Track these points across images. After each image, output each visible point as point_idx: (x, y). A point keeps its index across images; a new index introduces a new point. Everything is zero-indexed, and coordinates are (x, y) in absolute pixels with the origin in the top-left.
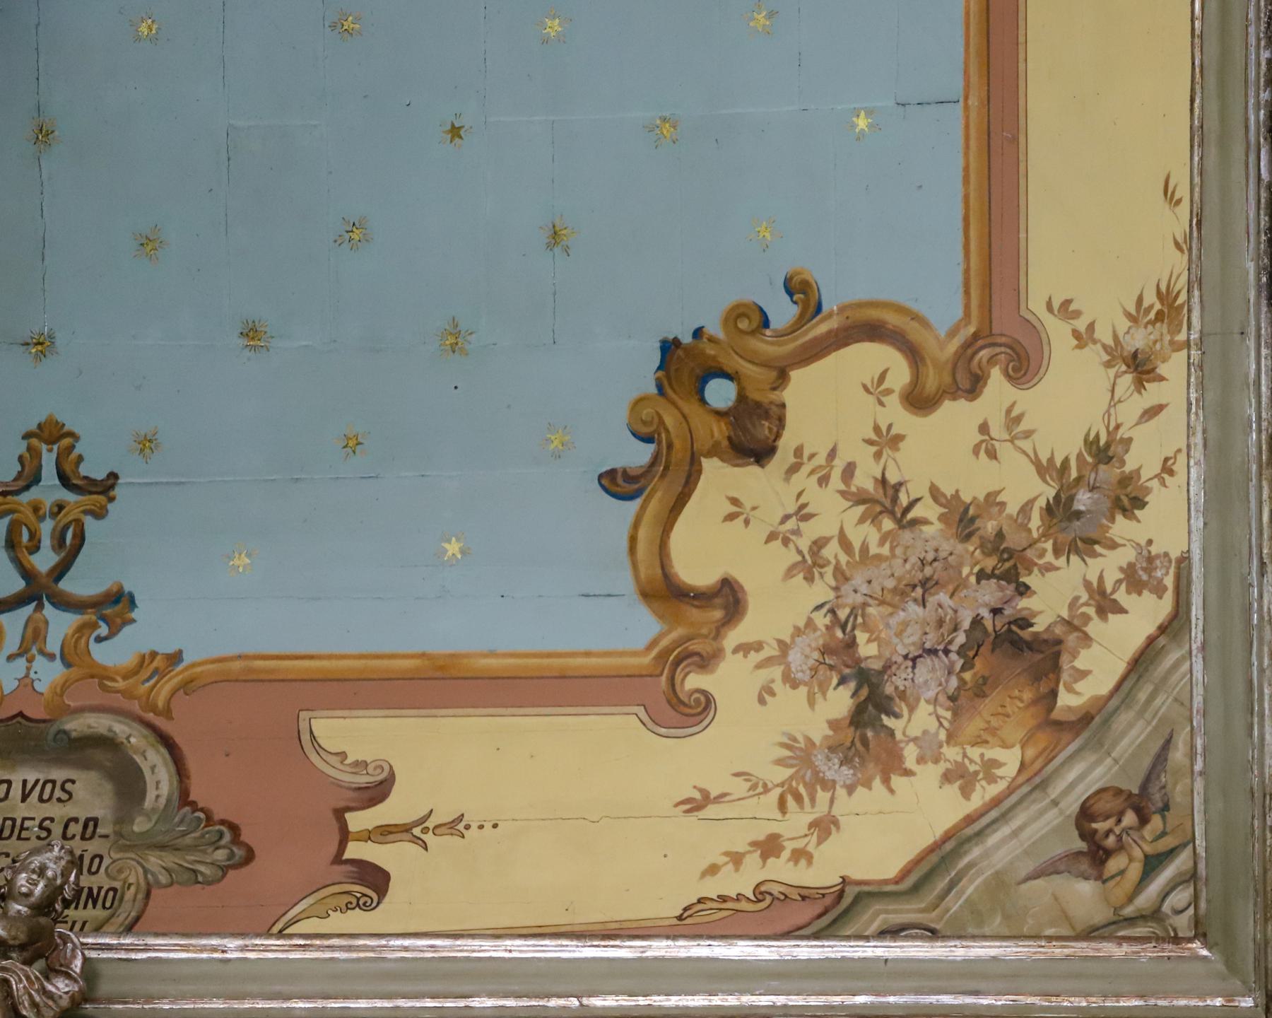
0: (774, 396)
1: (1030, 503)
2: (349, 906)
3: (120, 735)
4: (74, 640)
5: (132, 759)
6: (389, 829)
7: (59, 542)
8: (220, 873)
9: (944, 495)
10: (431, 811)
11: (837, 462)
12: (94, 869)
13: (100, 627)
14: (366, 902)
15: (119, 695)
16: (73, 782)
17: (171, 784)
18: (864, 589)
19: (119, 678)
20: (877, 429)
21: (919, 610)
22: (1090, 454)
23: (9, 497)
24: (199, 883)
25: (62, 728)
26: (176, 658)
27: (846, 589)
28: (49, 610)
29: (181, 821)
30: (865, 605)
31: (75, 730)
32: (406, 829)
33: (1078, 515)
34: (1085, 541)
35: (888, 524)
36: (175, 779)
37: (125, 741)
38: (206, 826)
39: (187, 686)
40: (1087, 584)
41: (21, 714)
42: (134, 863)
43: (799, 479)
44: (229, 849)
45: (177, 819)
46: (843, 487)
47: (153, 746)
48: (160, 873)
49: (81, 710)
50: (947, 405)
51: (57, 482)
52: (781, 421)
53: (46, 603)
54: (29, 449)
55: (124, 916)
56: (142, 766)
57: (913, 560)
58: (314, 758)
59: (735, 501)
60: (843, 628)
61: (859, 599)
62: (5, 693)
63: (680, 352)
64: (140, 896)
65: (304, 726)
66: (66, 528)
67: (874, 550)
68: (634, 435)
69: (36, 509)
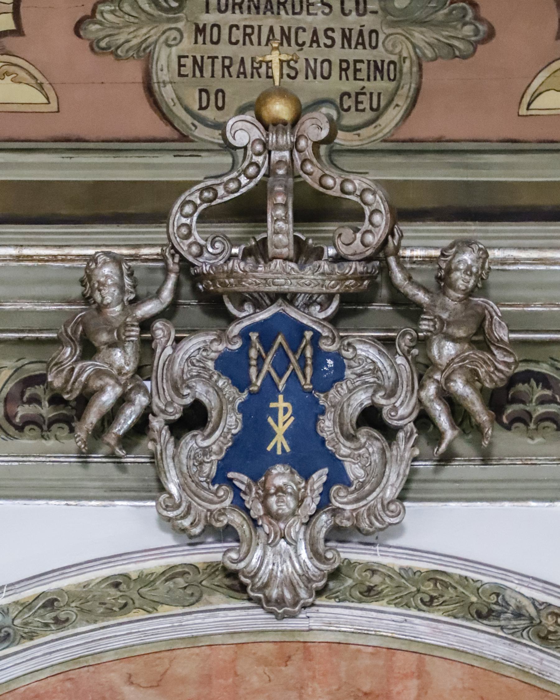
42: (403, 38)
44: (474, 25)
48: (425, 47)
55: (407, 87)
64: (415, 69)
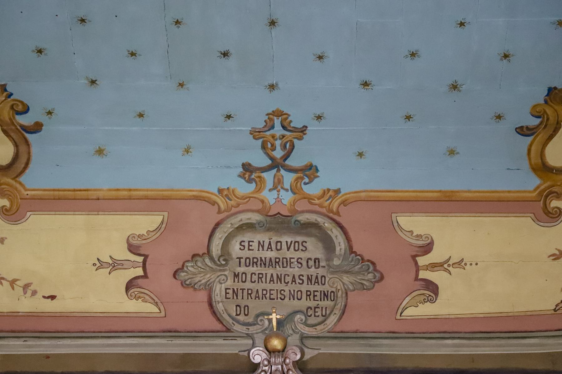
2: (425, 301)
3: (321, 222)
4: (295, 183)
5: (327, 232)
6: (434, 265)
7: (284, 147)
8: (372, 285)
10: (450, 257)
12: (323, 283)
13: (305, 179)
14: (431, 299)
15: (317, 206)
16: (306, 242)
17: (345, 244)
19: (316, 199)
23: (262, 133)
24: (365, 289)
25: (296, 219)
26: (338, 191)
28: (282, 172)
29: (352, 260)
31: (302, 220)
32: (441, 265)
36: (346, 241)
37: (323, 225)
38: (362, 263)
39: (344, 203)
41: (279, 213)
42: (338, 280)
45: (350, 259)
47: (334, 227)
49: (303, 212)
51: (281, 128)
53: (281, 169)
54: (269, 118)
55: (340, 304)
56: (332, 236)
58: (400, 233)
62: (271, 205)
63: (557, 91)
64: (344, 295)
65: (394, 219)
66: (287, 142)
68: (533, 116)
69: (273, 137)
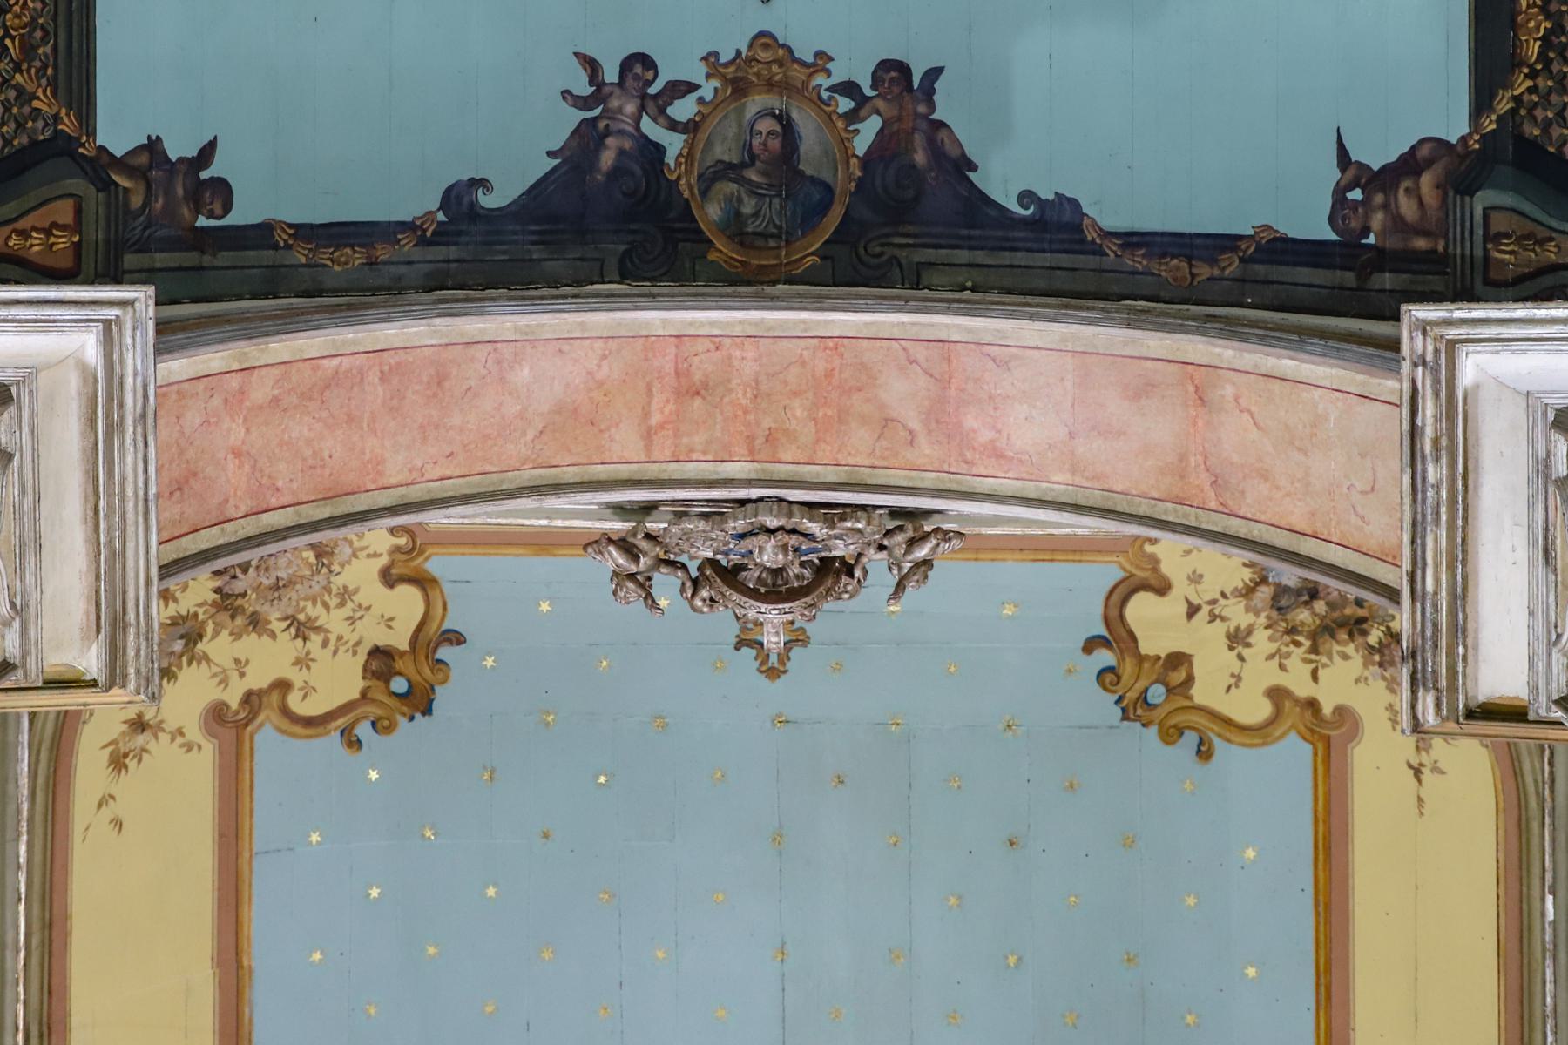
0: (369, 683)
1: (214, 637)
9: (268, 635)
11: (333, 648)
18: (313, 583)
20: (308, 667)
21: (280, 574)
22: (174, 672)
27: (324, 583)
30: (312, 575)
33: (182, 637)
34: (178, 624)
35: (301, 617)
40: (176, 600)
43: (354, 638)
46: (329, 635)
50: (264, 684)
52: (365, 669)
54: (784, 664)
57: (285, 600)
59: (390, 627)
60: (323, 564)
61: (316, 578)
63: (422, 708)
67: (309, 604)
68: (447, 664)
